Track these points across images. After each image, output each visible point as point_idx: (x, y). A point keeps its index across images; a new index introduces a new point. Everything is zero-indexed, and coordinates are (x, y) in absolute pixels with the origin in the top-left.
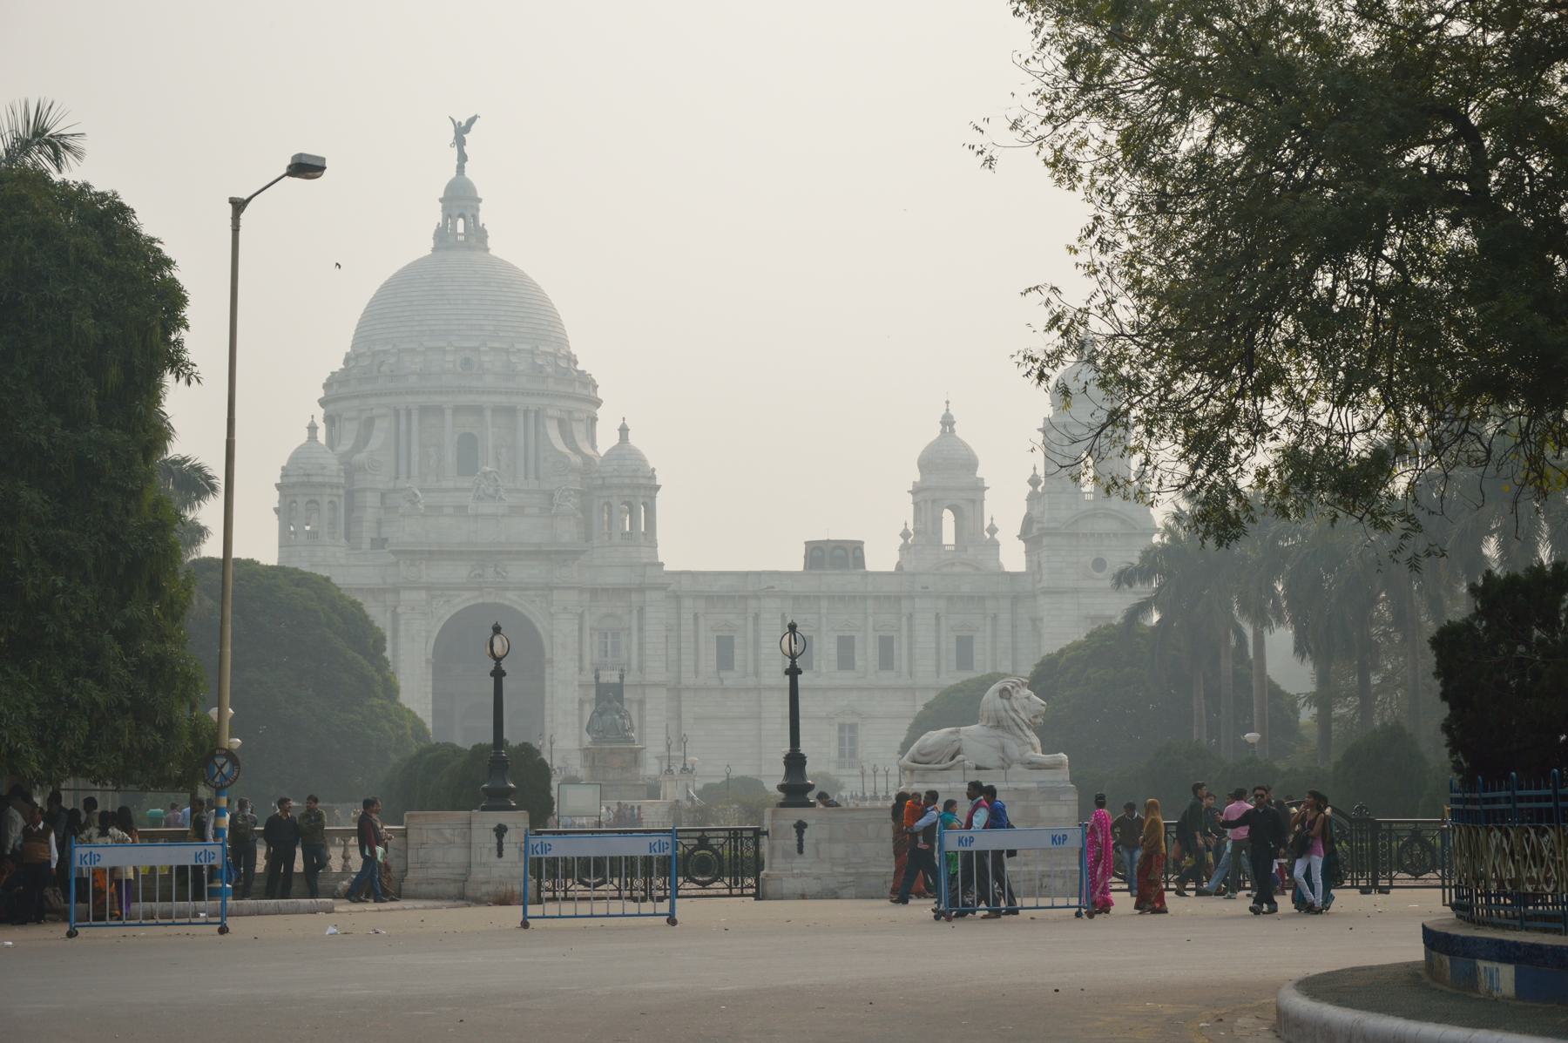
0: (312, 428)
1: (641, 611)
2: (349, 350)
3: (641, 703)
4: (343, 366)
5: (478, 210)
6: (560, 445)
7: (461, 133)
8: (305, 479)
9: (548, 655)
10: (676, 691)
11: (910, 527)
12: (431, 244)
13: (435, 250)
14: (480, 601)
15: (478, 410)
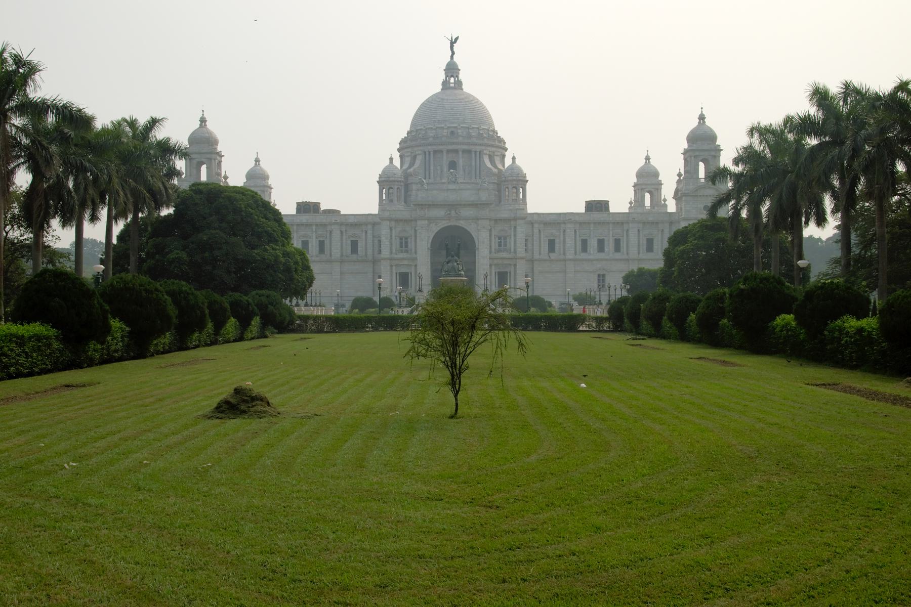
0: (391, 159)
1: (515, 228)
2: (409, 130)
3: (515, 265)
4: (406, 136)
5: (459, 73)
6: (489, 165)
7: (453, 43)
8: (388, 179)
9: (477, 247)
10: (532, 261)
11: (633, 199)
12: (441, 87)
13: (442, 89)
14: (450, 224)
15: (456, 151)
